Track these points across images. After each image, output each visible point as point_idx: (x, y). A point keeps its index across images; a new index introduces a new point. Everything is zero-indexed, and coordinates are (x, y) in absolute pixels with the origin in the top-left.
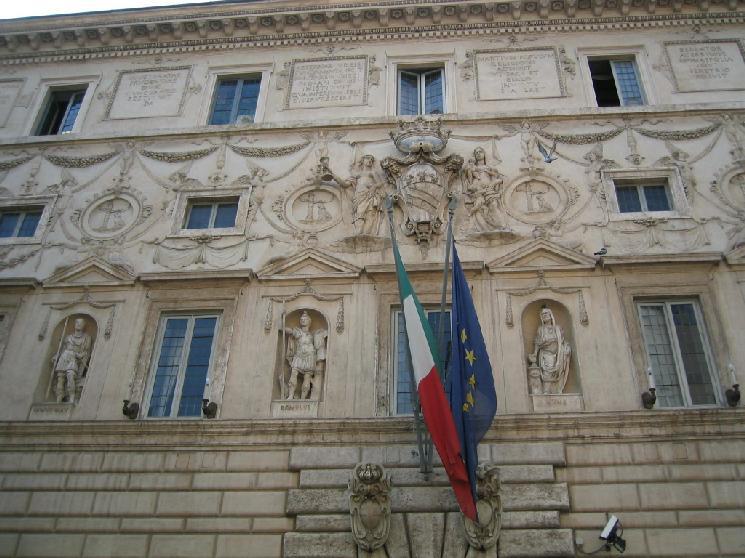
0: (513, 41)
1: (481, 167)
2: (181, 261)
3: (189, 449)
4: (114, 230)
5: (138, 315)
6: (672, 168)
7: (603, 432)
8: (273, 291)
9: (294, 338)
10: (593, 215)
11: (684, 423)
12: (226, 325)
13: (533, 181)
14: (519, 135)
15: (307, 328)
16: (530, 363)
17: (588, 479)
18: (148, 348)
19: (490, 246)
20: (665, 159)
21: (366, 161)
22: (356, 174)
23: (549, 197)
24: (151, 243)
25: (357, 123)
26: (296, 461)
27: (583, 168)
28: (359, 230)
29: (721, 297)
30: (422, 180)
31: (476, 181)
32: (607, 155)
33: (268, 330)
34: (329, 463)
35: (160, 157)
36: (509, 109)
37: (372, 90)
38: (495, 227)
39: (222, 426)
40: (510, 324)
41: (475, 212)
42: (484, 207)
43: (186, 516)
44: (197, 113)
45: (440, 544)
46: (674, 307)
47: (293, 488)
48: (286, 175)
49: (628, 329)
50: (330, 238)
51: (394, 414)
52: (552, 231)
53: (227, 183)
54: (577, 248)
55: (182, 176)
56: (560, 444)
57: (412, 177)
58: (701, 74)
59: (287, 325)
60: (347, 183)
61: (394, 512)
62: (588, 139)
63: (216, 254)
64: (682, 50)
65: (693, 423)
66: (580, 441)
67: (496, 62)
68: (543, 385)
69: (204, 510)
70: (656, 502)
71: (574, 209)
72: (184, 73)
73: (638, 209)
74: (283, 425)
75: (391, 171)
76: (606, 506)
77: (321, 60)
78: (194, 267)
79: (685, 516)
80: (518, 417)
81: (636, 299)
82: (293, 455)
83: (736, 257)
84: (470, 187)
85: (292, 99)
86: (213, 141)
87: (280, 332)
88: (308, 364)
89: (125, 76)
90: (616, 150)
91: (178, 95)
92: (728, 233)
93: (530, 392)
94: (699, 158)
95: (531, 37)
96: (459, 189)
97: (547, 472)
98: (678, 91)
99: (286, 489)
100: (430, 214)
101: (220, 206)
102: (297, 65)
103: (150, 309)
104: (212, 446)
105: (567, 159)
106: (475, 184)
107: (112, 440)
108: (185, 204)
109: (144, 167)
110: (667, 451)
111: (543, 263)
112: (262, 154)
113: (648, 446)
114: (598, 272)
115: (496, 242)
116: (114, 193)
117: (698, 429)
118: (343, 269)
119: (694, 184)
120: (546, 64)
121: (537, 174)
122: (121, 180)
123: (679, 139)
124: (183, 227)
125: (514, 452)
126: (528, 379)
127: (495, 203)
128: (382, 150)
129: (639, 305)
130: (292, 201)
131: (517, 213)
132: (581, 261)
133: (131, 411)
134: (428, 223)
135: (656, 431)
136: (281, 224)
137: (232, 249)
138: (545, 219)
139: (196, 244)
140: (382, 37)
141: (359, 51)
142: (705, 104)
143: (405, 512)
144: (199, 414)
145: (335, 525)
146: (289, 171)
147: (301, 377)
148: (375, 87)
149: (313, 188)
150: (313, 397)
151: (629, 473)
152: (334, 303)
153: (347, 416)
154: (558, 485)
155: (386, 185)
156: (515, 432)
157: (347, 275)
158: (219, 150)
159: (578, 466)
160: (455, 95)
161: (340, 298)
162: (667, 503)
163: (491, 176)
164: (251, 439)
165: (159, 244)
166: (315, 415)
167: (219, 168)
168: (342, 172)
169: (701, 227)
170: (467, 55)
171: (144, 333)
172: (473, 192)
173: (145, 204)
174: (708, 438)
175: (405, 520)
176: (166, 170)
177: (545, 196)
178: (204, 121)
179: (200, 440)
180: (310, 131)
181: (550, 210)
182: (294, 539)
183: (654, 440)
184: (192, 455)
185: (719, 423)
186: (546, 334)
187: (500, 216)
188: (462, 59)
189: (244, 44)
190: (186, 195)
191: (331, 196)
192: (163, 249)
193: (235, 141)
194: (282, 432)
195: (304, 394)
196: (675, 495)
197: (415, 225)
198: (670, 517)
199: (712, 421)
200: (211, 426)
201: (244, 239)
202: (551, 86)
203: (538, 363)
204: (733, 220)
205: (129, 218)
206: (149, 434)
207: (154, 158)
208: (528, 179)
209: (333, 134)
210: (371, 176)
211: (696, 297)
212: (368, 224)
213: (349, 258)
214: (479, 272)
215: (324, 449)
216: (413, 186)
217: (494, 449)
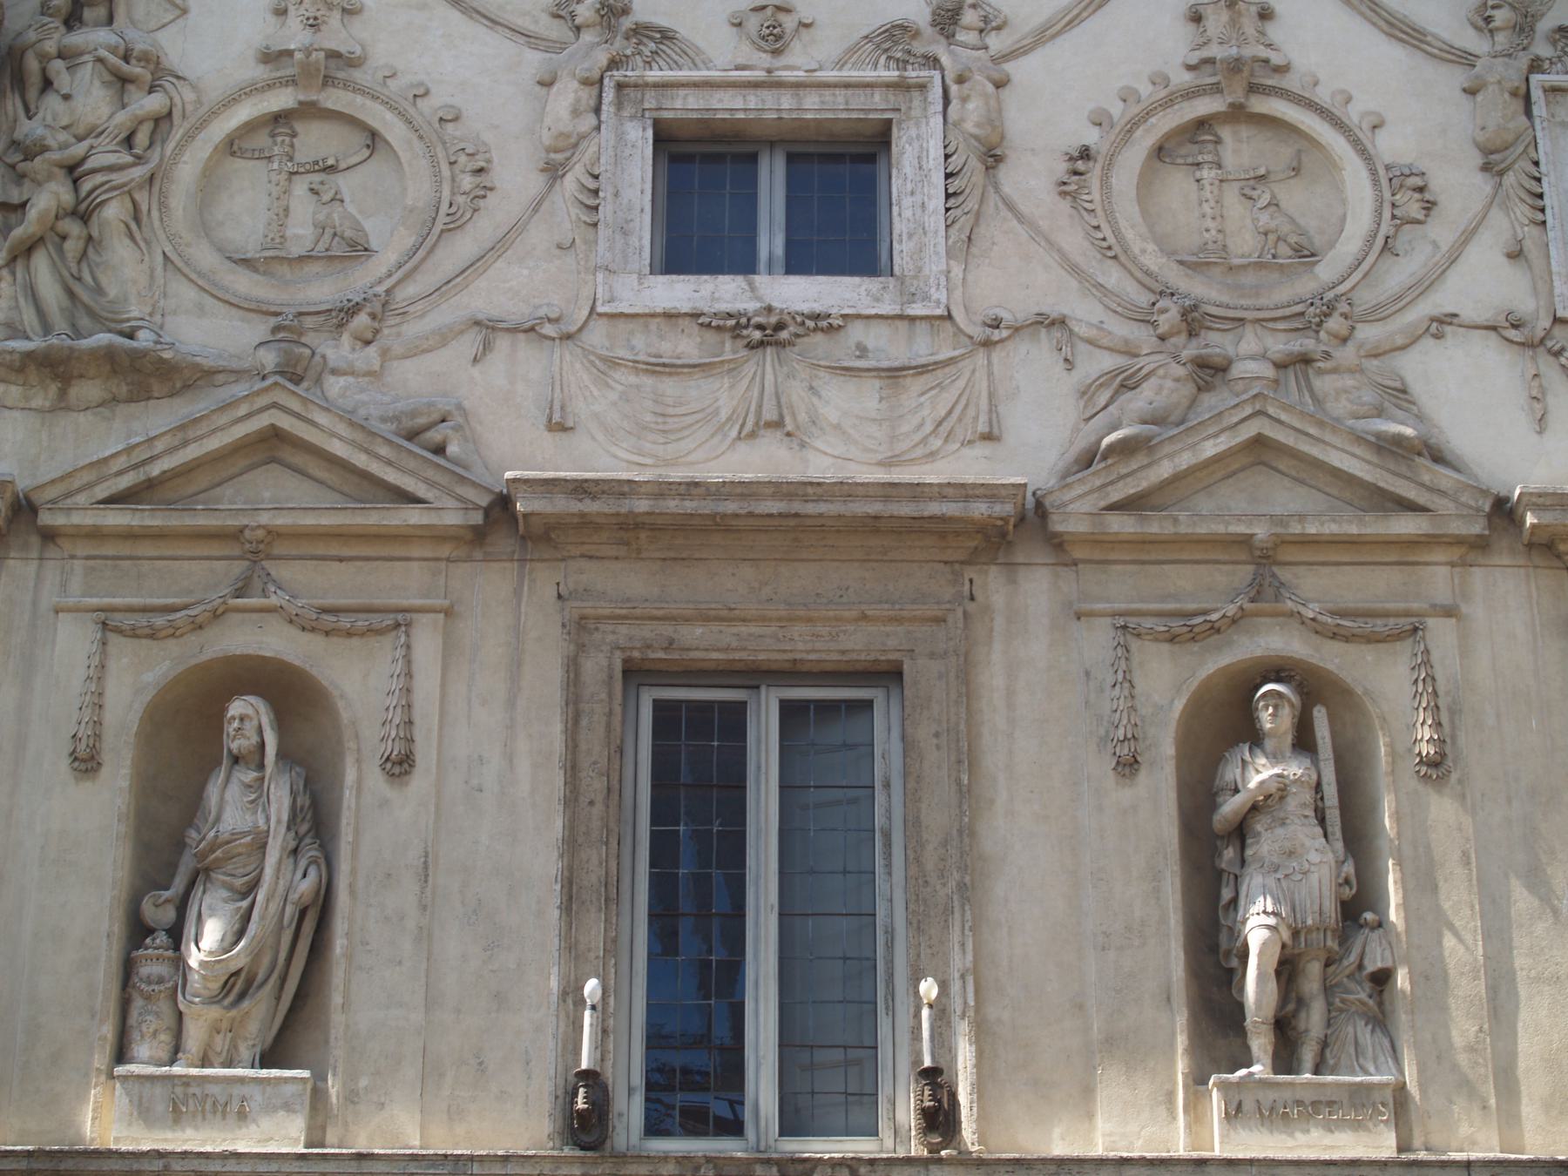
6: (912, 74)
10: (509, 289)
13: (310, 110)
16: (138, 931)
19: (62, 404)
27: (534, 61)
29: (992, 677)
31: (52, 102)
38: (101, 321)
41: (27, 250)
42: (73, 227)
46: (791, 712)
52: (338, 350)
54: (423, 435)
71: (463, 247)
73: (745, 264)
81: (635, 674)
83: (1086, 506)
84: (30, 129)
92: (1086, 393)
94: (1043, 36)
114: (503, 543)
115: (88, 390)
119: (993, 158)
121: (328, 81)
127: (114, 211)
131: (205, 257)
132: (420, 490)
138: (322, 290)
163: (123, 81)
169: (981, 358)
172: (29, 156)
181: (359, 249)
204: (1122, 330)
208: (283, 99)
211: (890, 675)
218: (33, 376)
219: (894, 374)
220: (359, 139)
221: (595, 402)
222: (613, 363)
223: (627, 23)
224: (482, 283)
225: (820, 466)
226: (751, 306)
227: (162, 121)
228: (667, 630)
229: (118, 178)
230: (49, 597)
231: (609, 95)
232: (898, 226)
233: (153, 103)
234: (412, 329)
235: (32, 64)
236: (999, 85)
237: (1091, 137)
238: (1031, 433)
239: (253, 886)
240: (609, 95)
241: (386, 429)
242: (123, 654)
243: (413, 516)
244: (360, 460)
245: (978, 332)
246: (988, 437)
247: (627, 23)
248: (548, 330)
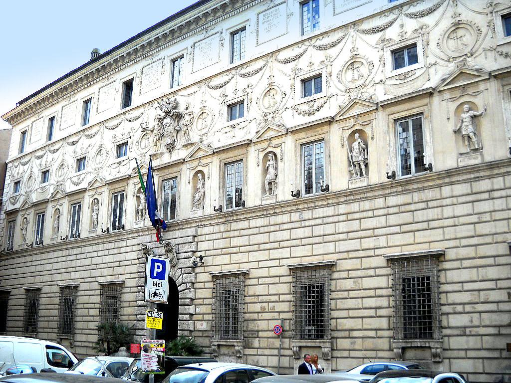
3: (119, 241)
19: (187, 149)
42: (187, 131)
97: (190, 239)
110: (222, 228)
115: (188, 147)
125: (177, 233)
174: (234, 221)
185: (237, 215)
214: (182, 163)
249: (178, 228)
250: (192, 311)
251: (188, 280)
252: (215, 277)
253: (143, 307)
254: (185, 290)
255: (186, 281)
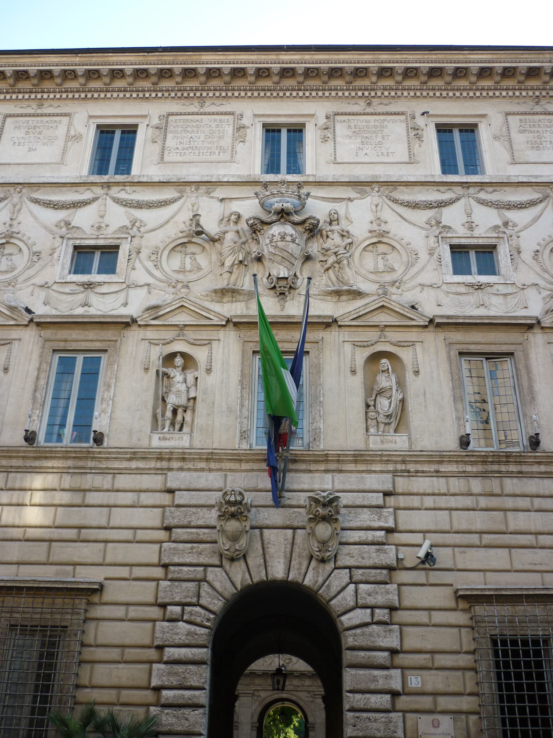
0: (369, 104)
1: (335, 227)
2: (69, 305)
4: (6, 272)
5: (32, 351)
6: (501, 235)
7: (426, 468)
8: (150, 334)
9: (168, 377)
10: (427, 277)
11: (492, 463)
12: (110, 364)
13: (380, 242)
14: (369, 198)
15: (180, 368)
16: (368, 406)
17: (411, 505)
18: (42, 382)
19: (339, 301)
20: (496, 227)
21: (233, 217)
22: (223, 229)
23: (392, 258)
24: (42, 286)
25: (225, 180)
26: (171, 484)
27: (424, 233)
28: (226, 282)
29: (533, 355)
30: (283, 238)
31: (329, 240)
32: (445, 221)
33: (146, 369)
34: (200, 486)
35: (49, 205)
36: (362, 173)
37: (240, 147)
39: (109, 453)
40: (354, 372)
41: (328, 269)
43: (80, 528)
44: (79, 162)
45: (288, 555)
47: (169, 506)
48: (162, 226)
49: (452, 380)
50: (201, 288)
51: (254, 447)
52: (393, 290)
53: (109, 232)
55: (67, 224)
56: (390, 476)
57: (273, 236)
58: (536, 146)
59: (164, 366)
60: (217, 237)
61: (252, 528)
62: (429, 206)
63: (100, 298)
64: (521, 120)
65: (499, 463)
66: (406, 474)
67: (353, 125)
68: (378, 426)
69: (95, 524)
70: (464, 526)
71: (414, 270)
72: (65, 120)
73: (470, 273)
74: (160, 453)
75: (257, 227)
76: (425, 528)
77: (193, 114)
78: (80, 311)
79: (487, 539)
80: (356, 453)
81: (461, 354)
82: (169, 479)
84: (325, 246)
85: (166, 153)
86: (94, 191)
87: (157, 372)
88: (183, 401)
89: (9, 120)
90: (453, 216)
91: (60, 143)
92: (544, 299)
93: (367, 430)
94: (525, 228)
95: (386, 101)
96: (314, 248)
97: (378, 499)
98: (514, 162)
99: (163, 507)
100: (289, 270)
101: (102, 253)
102: (171, 118)
103: (43, 348)
104: (101, 468)
105: (410, 223)
106: (329, 244)
107: (15, 463)
108: (71, 250)
109: (31, 213)
110: (476, 485)
111: (383, 318)
112: (139, 205)
113: (462, 480)
114: (431, 328)
115: (344, 298)
116: (4, 238)
117: (503, 468)
118: (212, 317)
119: (519, 252)
120: (397, 128)
121: (383, 236)
122: (11, 226)
123: (509, 209)
124: (70, 273)
126: (366, 420)
127: (345, 262)
128: (249, 207)
129: (463, 359)
130: (166, 252)
131: (363, 272)
133: (30, 437)
134: (287, 278)
135: (469, 468)
136: (157, 273)
137: (114, 295)
138: (388, 278)
139: (82, 289)
140: (249, 94)
141: (228, 107)
142: (537, 177)
143: (261, 528)
144: (88, 442)
145: (205, 538)
146: (166, 222)
147: (175, 412)
148: (242, 144)
149: (185, 240)
150: (186, 429)
151: (442, 502)
152: (203, 348)
153: (214, 447)
154: (385, 510)
155: (250, 241)
156: (353, 465)
157: (215, 323)
158: (100, 200)
159: (403, 494)
160: (316, 158)
161: (209, 342)
162: (473, 528)
164: (134, 464)
165: (48, 287)
166: (187, 445)
167: (102, 217)
168: (211, 226)
170: (327, 117)
171: (39, 369)
173: (35, 249)
174: (510, 475)
175: (262, 535)
176: (53, 217)
177: (388, 257)
178: (85, 171)
179: (90, 464)
180: (182, 184)
181: (393, 270)
182: (170, 549)
183: (465, 475)
184: (84, 476)
186: (383, 381)
187: (349, 274)
188: (322, 121)
189: (121, 95)
190: (71, 242)
191: (202, 248)
192: (52, 292)
193: (115, 191)
194: (160, 459)
195: (177, 427)
196: (479, 521)
197: (275, 280)
198: (474, 539)
199: (516, 462)
200: (100, 453)
201: (124, 286)
202: (400, 152)
203: (374, 406)
205: (21, 261)
206: (46, 458)
207: (40, 205)
208: (375, 240)
209: (203, 189)
210: (238, 232)
212: (234, 277)
213: (217, 307)
214: (328, 325)
215: (195, 474)
216: (274, 244)
217: (336, 478)
218: (333, 295)
219: (505, 295)
220: (390, 248)
221: (445, 300)
222: (449, 293)
223: (441, 225)
224: (419, 277)
225: (493, 312)
226: (475, 282)
227: (351, 244)
228: (466, 346)
229: (345, 255)
230: (341, 339)
231: (440, 239)
232: (501, 266)
233: (349, 241)
234: (407, 286)
235: (324, 233)
236: (518, 237)
237: (538, 248)
238: (534, 307)
239: (391, 397)
240: (440, 239)
241: (407, 305)
242: (358, 351)
243: (414, 323)
244: (402, 312)
245: (521, 287)
246: (525, 308)
247: (441, 225)
248: (435, 286)
249: (322, 467)
250: (397, 685)
251: (380, 599)
252: (469, 599)
253: (191, 667)
254: (366, 625)
255: (370, 601)
